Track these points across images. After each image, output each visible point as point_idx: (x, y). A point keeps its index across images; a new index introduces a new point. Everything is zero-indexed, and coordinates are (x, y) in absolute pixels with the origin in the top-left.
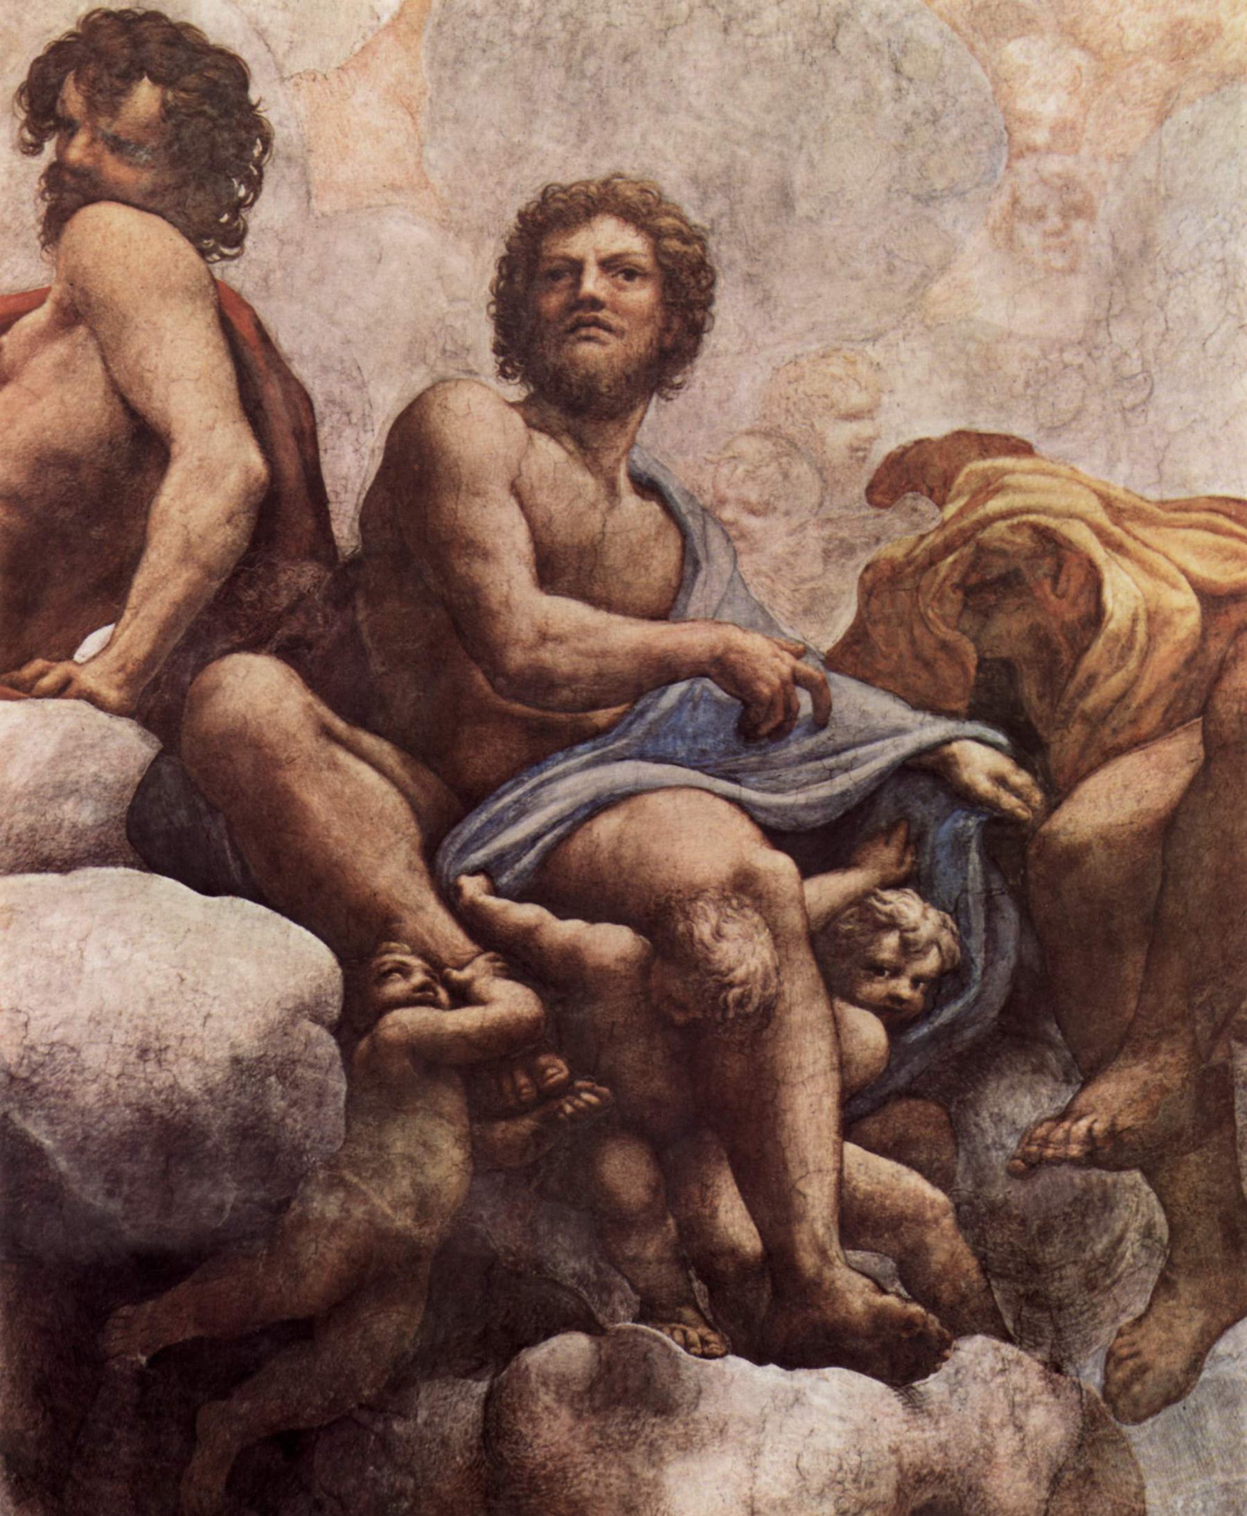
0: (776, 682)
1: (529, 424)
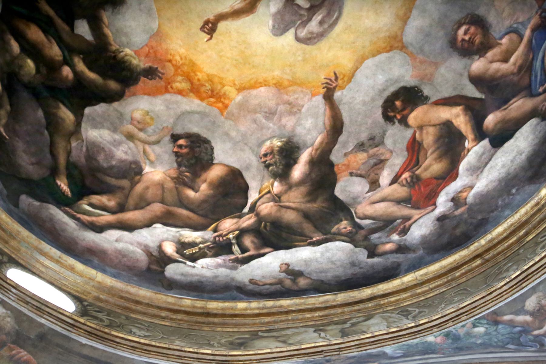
0: (539, 19)
1: (483, 57)
